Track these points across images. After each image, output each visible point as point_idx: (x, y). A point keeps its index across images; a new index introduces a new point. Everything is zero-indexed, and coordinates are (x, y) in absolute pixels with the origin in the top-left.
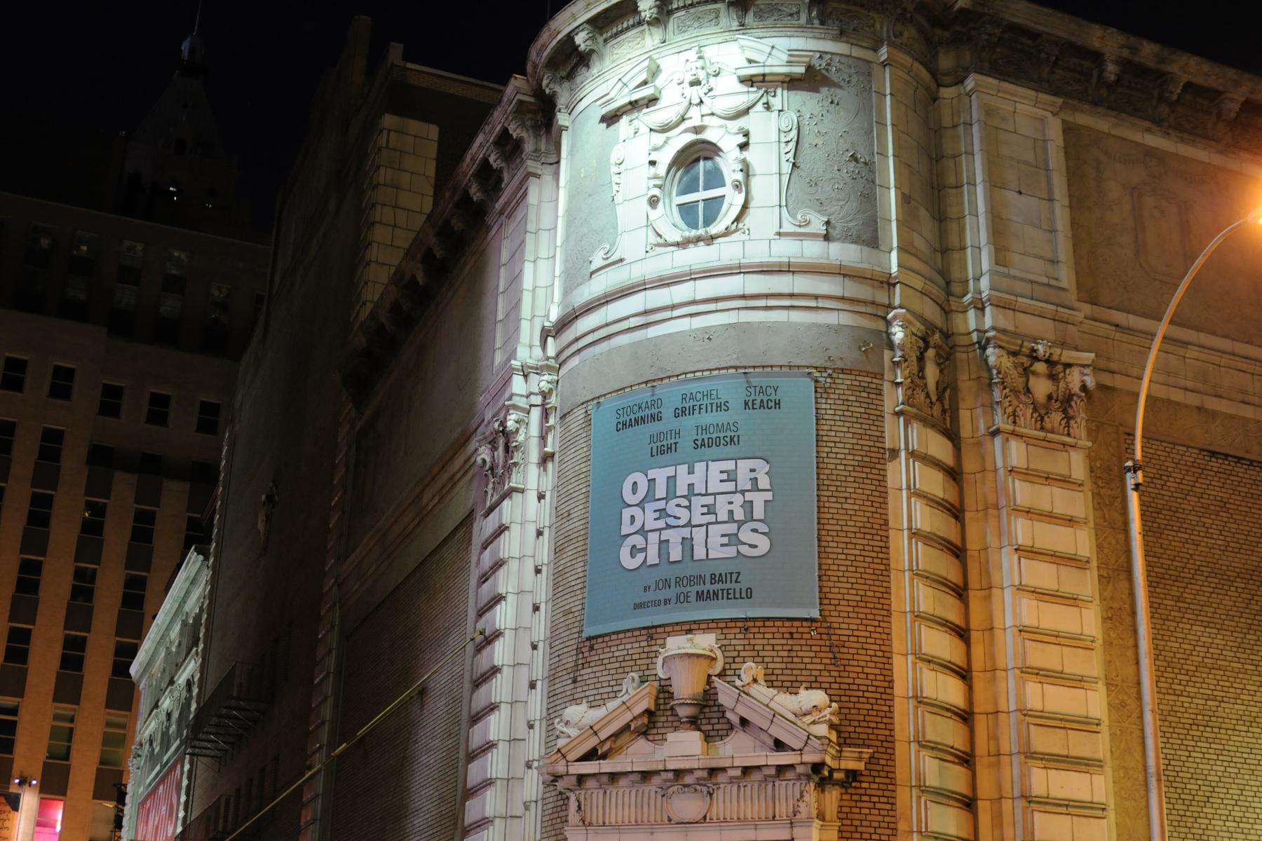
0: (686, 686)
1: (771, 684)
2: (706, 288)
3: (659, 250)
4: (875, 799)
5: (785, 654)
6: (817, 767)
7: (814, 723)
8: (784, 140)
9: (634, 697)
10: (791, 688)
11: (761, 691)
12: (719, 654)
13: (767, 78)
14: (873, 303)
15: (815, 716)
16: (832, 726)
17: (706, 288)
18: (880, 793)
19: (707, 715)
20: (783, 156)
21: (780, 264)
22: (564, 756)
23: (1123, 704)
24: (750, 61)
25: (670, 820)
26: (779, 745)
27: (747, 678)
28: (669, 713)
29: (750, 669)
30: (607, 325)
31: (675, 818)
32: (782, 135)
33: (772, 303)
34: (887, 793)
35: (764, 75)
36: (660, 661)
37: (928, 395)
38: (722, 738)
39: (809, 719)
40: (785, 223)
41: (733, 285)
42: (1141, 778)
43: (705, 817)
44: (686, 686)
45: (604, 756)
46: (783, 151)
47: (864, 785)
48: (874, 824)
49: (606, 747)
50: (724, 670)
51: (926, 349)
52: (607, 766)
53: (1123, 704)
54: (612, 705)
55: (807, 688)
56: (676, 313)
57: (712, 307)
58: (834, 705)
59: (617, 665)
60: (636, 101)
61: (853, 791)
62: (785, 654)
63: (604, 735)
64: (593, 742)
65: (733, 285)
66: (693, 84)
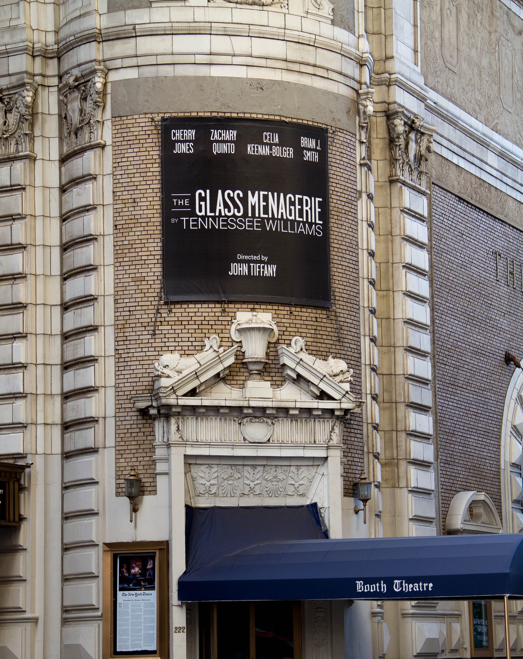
5: (313, 332)
7: (341, 382)
11: (308, 358)
12: (275, 328)
15: (340, 378)
17: (261, 47)
19: (271, 368)
25: (245, 439)
26: (323, 396)
28: (241, 366)
36: (233, 327)
39: (338, 379)
41: (277, 49)
43: (269, 440)
44: (255, 349)
50: (278, 339)
55: (334, 357)
56: (236, 60)
57: (262, 62)
58: (352, 370)
59: (196, 327)
62: (313, 332)
65: (277, 49)
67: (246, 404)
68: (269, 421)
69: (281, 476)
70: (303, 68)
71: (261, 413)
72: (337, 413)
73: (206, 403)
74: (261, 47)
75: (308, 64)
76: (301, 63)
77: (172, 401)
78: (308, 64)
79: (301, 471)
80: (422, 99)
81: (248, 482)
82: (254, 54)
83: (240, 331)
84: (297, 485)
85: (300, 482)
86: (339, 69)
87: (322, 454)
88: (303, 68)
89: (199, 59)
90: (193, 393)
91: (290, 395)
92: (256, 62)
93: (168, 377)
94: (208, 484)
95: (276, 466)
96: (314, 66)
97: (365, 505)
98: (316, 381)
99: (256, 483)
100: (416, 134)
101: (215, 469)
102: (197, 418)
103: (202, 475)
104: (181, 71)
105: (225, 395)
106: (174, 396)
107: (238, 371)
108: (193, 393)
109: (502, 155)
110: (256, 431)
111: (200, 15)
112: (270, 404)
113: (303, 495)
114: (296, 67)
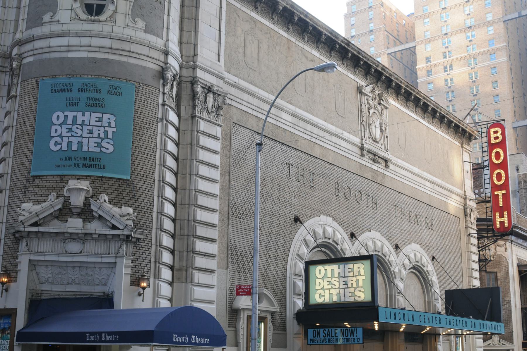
0: (78, 201)
1: (110, 203)
3: (77, 21)
4: (144, 249)
5: (116, 192)
6: (128, 236)
7: (128, 219)
9: (52, 203)
10: (118, 205)
11: (108, 206)
12: (91, 189)
15: (128, 217)
16: (134, 221)
17: (96, 42)
18: (146, 247)
19: (86, 213)
22: (23, 224)
23: (223, 220)
25: (66, 252)
26: (114, 227)
27: (102, 200)
28: (68, 210)
29: (104, 197)
31: (69, 251)
34: (148, 247)
36: (65, 189)
37: (173, 99)
38: (90, 222)
39: (125, 218)
42: (226, 246)
43: (81, 252)
44: (78, 201)
45: (39, 225)
47: (141, 244)
48: (144, 258)
49: (41, 222)
50: (92, 195)
51: (174, 80)
52: (42, 229)
53: (223, 220)
54: (43, 205)
55: (125, 206)
56: (82, 49)
57: (97, 49)
58: (136, 214)
59: (46, 189)
61: (136, 245)
62: (116, 192)
63: (41, 217)
64: (36, 219)
65: (107, 43)
67: (65, 231)
68: (82, 241)
69: (91, 273)
70: (122, 53)
71: (73, 237)
72: (121, 237)
73: (47, 230)
74: (96, 42)
75: (125, 51)
76: (120, 50)
77: (21, 228)
78: (125, 51)
79: (102, 270)
80: (222, 78)
81: (71, 276)
82: (92, 45)
83: (69, 190)
84: (100, 278)
85: (103, 277)
86: (147, 54)
87: (113, 260)
88: (122, 53)
89: (62, 49)
90: (35, 224)
91: (95, 227)
92: (93, 49)
93: (24, 216)
94: (46, 277)
95: (87, 267)
96: (130, 52)
97: (144, 291)
98: (109, 219)
99: (75, 277)
100: (213, 95)
101: (50, 268)
102: (39, 239)
103: (42, 271)
104: (53, 55)
105: (56, 226)
106: (23, 226)
107: (65, 212)
108: (35, 224)
109: (294, 115)
110: (74, 247)
111: (65, 28)
112: (80, 231)
113: (105, 284)
114: (118, 52)
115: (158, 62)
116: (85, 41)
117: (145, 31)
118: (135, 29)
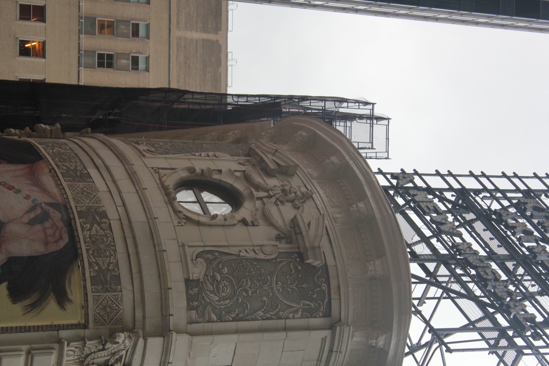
2: (132, 200)
8: (256, 249)
13: (299, 235)
14: (144, 317)
17: (132, 200)
20: (243, 248)
21: (160, 244)
24: (309, 225)
30: (94, 150)
32: (259, 248)
33: (130, 241)
35: (301, 233)
40: (192, 250)
46: (247, 248)
60: (263, 161)
66: (283, 191)
96: (137, 254)
115: (139, 314)
116: (125, 185)
117: (188, 282)
118: (183, 260)
